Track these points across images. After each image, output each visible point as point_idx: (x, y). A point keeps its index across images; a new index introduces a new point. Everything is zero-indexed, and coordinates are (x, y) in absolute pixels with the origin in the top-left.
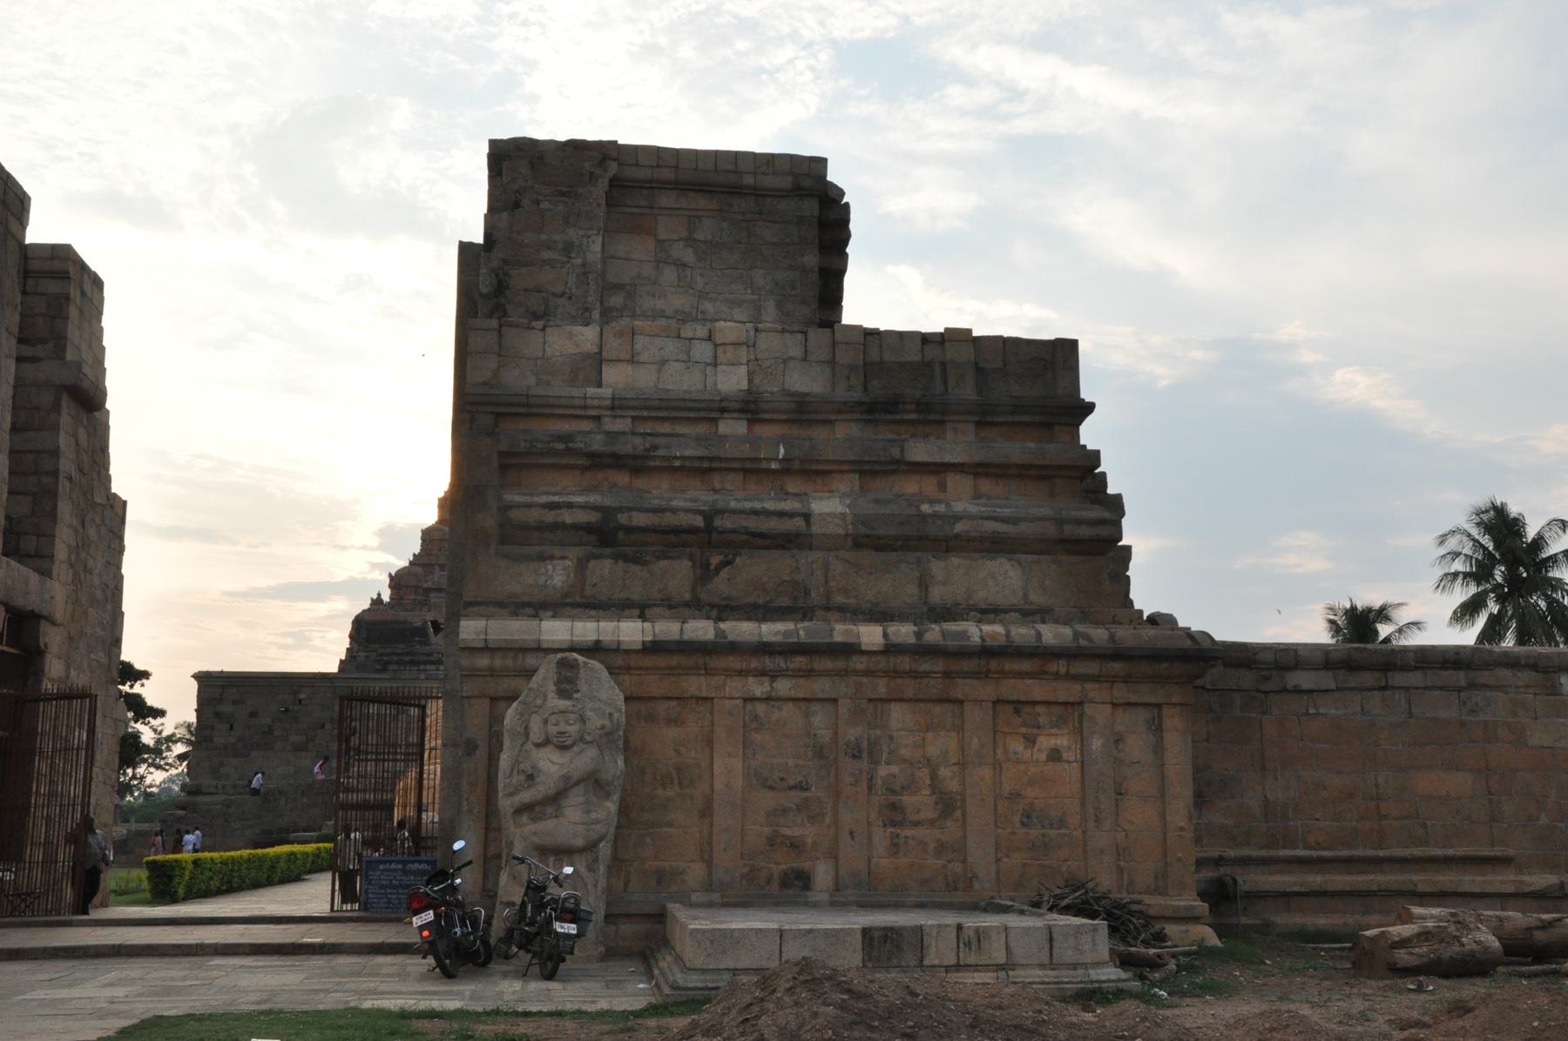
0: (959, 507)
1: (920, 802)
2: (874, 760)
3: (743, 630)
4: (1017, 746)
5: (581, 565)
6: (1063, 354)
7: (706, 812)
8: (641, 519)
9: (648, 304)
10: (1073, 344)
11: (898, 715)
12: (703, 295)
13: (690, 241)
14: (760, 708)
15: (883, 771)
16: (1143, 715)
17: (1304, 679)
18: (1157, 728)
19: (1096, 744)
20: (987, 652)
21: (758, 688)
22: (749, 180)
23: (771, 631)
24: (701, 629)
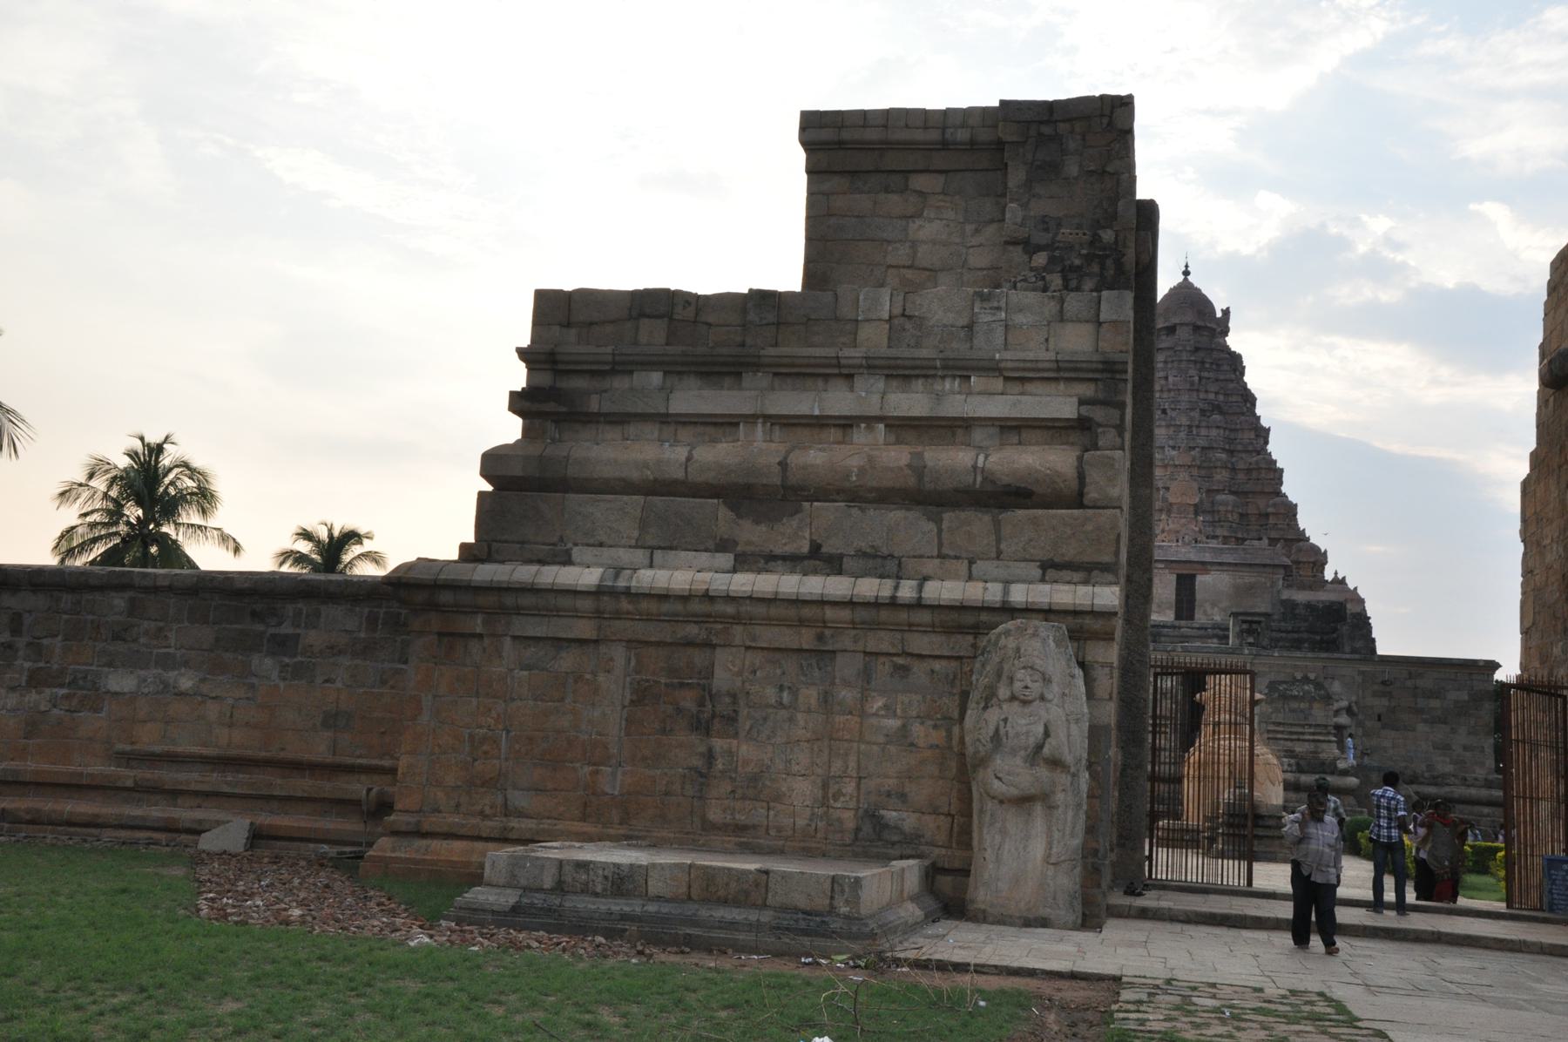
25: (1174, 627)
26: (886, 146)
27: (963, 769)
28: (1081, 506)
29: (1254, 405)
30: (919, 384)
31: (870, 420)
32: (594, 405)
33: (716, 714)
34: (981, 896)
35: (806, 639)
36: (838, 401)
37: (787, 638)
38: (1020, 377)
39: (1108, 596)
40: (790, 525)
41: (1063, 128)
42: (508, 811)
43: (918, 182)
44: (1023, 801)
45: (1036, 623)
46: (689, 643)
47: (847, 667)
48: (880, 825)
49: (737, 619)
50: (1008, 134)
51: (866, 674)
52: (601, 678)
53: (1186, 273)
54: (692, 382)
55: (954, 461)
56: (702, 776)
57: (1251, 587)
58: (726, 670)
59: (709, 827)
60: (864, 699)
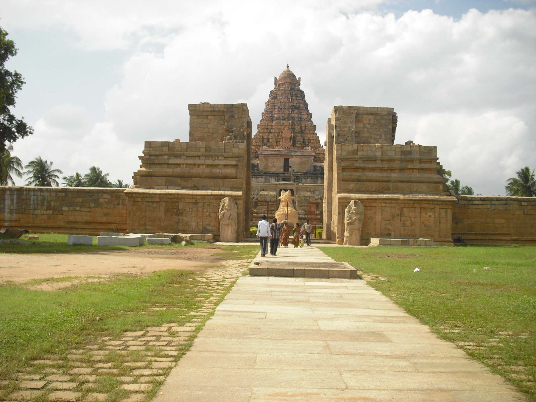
1: (408, 223)
2: (401, 217)
4: (424, 215)
7: (375, 224)
8: (365, 178)
9: (362, 135)
10: (435, 148)
11: (405, 210)
12: (371, 134)
13: (369, 124)
14: (384, 208)
15: (402, 218)
16: (444, 210)
18: (446, 212)
19: (437, 214)
21: (383, 205)
22: (379, 113)
25: (283, 173)
26: (203, 111)
29: (307, 106)
30: (210, 158)
31: (203, 165)
32: (156, 161)
33: (179, 213)
34: (221, 239)
35: (194, 201)
36: (198, 161)
38: (227, 158)
39: (240, 193)
41: (234, 109)
43: (210, 117)
44: (228, 225)
46: (175, 202)
47: (200, 205)
48: (206, 229)
49: (182, 198)
51: (203, 206)
52: (161, 208)
53: (288, 67)
54: (173, 157)
55: (217, 171)
56: (178, 223)
60: (203, 210)
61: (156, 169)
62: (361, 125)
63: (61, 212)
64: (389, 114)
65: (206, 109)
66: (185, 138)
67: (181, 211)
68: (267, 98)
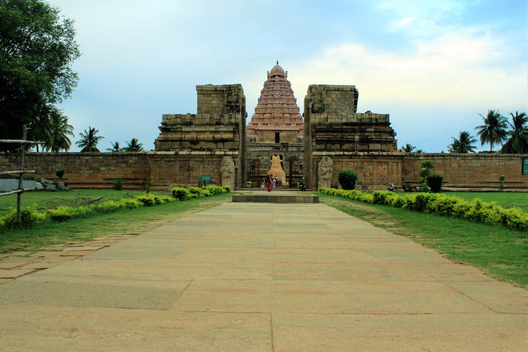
0: (373, 137)
3: (346, 153)
4: (380, 167)
5: (326, 146)
6: (387, 116)
9: (331, 107)
11: (365, 163)
13: (337, 98)
16: (395, 164)
17: (421, 158)
20: (376, 156)
21: (348, 160)
23: (351, 153)
24: (341, 153)
27: (220, 174)
28: (233, 141)
31: (208, 131)
35: (201, 159)
37: (198, 159)
40: (198, 145)
42: (165, 182)
43: (213, 95)
44: (227, 177)
45: (229, 157)
46: (186, 160)
47: (206, 162)
49: (192, 157)
50: (225, 89)
51: (208, 163)
53: (277, 63)
54: (184, 126)
55: (218, 136)
56: (189, 177)
57: (291, 135)
58: (191, 163)
59: (190, 183)
61: (170, 136)
62: (330, 99)
63: (99, 171)
64: (351, 90)
65: (209, 89)
66: (195, 112)
67: (191, 168)
68: (262, 87)
